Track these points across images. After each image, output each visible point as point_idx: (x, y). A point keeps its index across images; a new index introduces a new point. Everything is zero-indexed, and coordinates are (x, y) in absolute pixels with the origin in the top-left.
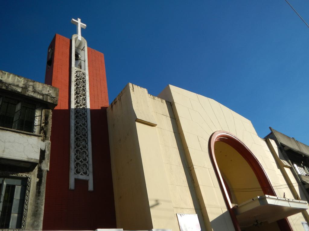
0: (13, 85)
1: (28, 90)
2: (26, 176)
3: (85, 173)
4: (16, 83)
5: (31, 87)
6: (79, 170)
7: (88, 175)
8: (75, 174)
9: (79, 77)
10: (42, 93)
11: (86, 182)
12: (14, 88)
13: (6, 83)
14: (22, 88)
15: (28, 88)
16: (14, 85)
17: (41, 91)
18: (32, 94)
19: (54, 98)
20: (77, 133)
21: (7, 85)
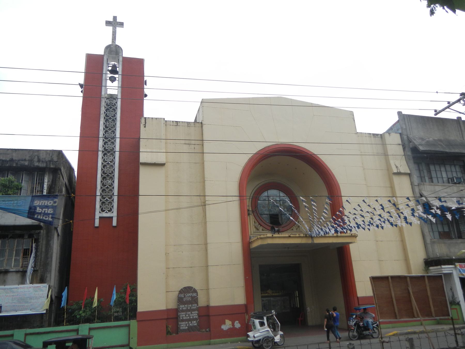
0: (22, 160)
1: (34, 161)
2: (38, 232)
3: (110, 211)
4: (24, 158)
5: (36, 157)
6: (104, 209)
7: (113, 212)
8: (100, 212)
9: (109, 106)
10: (46, 160)
11: (112, 218)
12: (22, 162)
13: (16, 160)
14: (29, 160)
15: (34, 159)
16: (22, 160)
17: (45, 159)
18: (36, 164)
19: (56, 162)
20: (104, 172)
21: (17, 162)
